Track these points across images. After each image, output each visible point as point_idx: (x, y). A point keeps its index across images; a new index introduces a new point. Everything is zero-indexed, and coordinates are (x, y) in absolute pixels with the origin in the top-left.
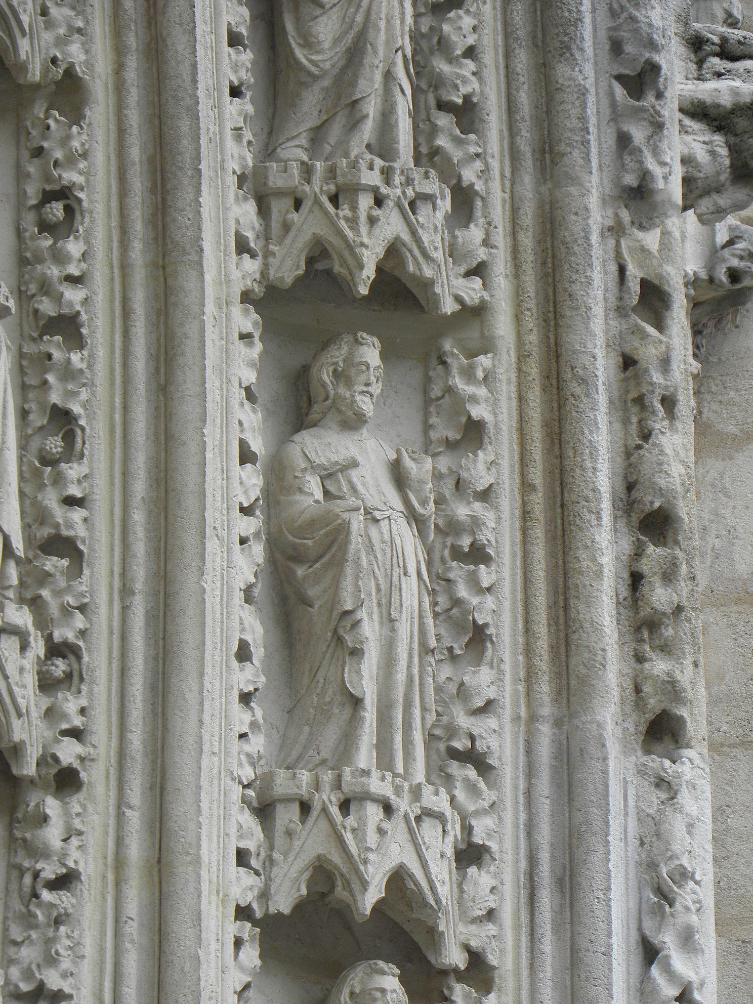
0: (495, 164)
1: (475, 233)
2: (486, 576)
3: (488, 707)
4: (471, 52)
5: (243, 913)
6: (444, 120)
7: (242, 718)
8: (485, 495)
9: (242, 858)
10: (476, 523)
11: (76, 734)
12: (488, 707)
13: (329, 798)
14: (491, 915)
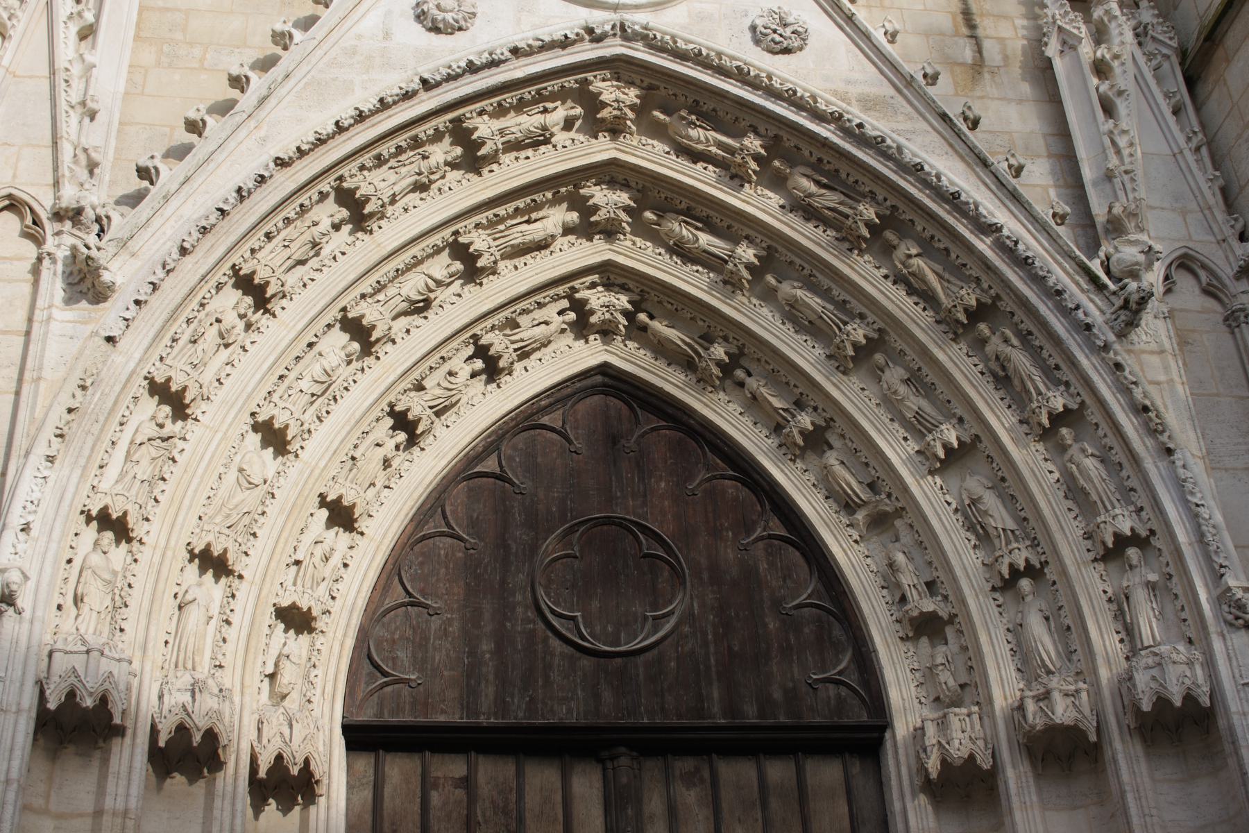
0: (1068, 372)
1: (1072, 388)
2: (1113, 452)
3: (1129, 477)
4: (1050, 356)
5: (1095, 560)
6: (1055, 372)
7: (1077, 523)
8: (1105, 436)
9: (1089, 550)
10: (1106, 444)
11: (1044, 553)
12: (1129, 477)
13: (1096, 528)
14: (1149, 519)
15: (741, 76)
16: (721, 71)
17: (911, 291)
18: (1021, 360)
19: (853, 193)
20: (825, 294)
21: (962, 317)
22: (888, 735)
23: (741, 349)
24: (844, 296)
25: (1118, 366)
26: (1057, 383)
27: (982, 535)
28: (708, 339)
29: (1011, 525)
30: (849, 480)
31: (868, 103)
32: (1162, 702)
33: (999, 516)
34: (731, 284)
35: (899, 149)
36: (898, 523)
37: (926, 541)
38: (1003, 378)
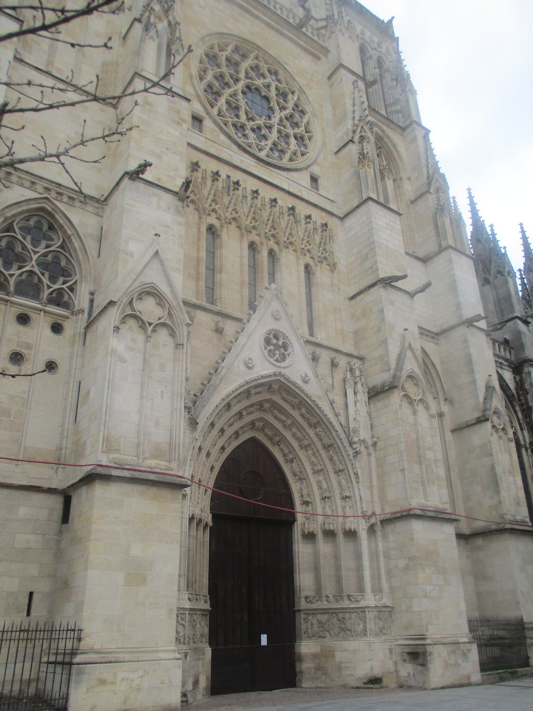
15: (299, 388)
16: (296, 387)
17: (318, 437)
18: (335, 458)
19: (312, 415)
20: (302, 433)
21: (326, 446)
22: (296, 523)
23: (281, 439)
24: (305, 435)
25: (352, 464)
26: (341, 463)
27: (320, 488)
28: (276, 435)
29: (326, 488)
30: (297, 470)
31: (319, 397)
32: (350, 530)
33: (325, 486)
34: (285, 426)
35: (324, 411)
36: (304, 481)
37: (309, 486)
38: (331, 459)
